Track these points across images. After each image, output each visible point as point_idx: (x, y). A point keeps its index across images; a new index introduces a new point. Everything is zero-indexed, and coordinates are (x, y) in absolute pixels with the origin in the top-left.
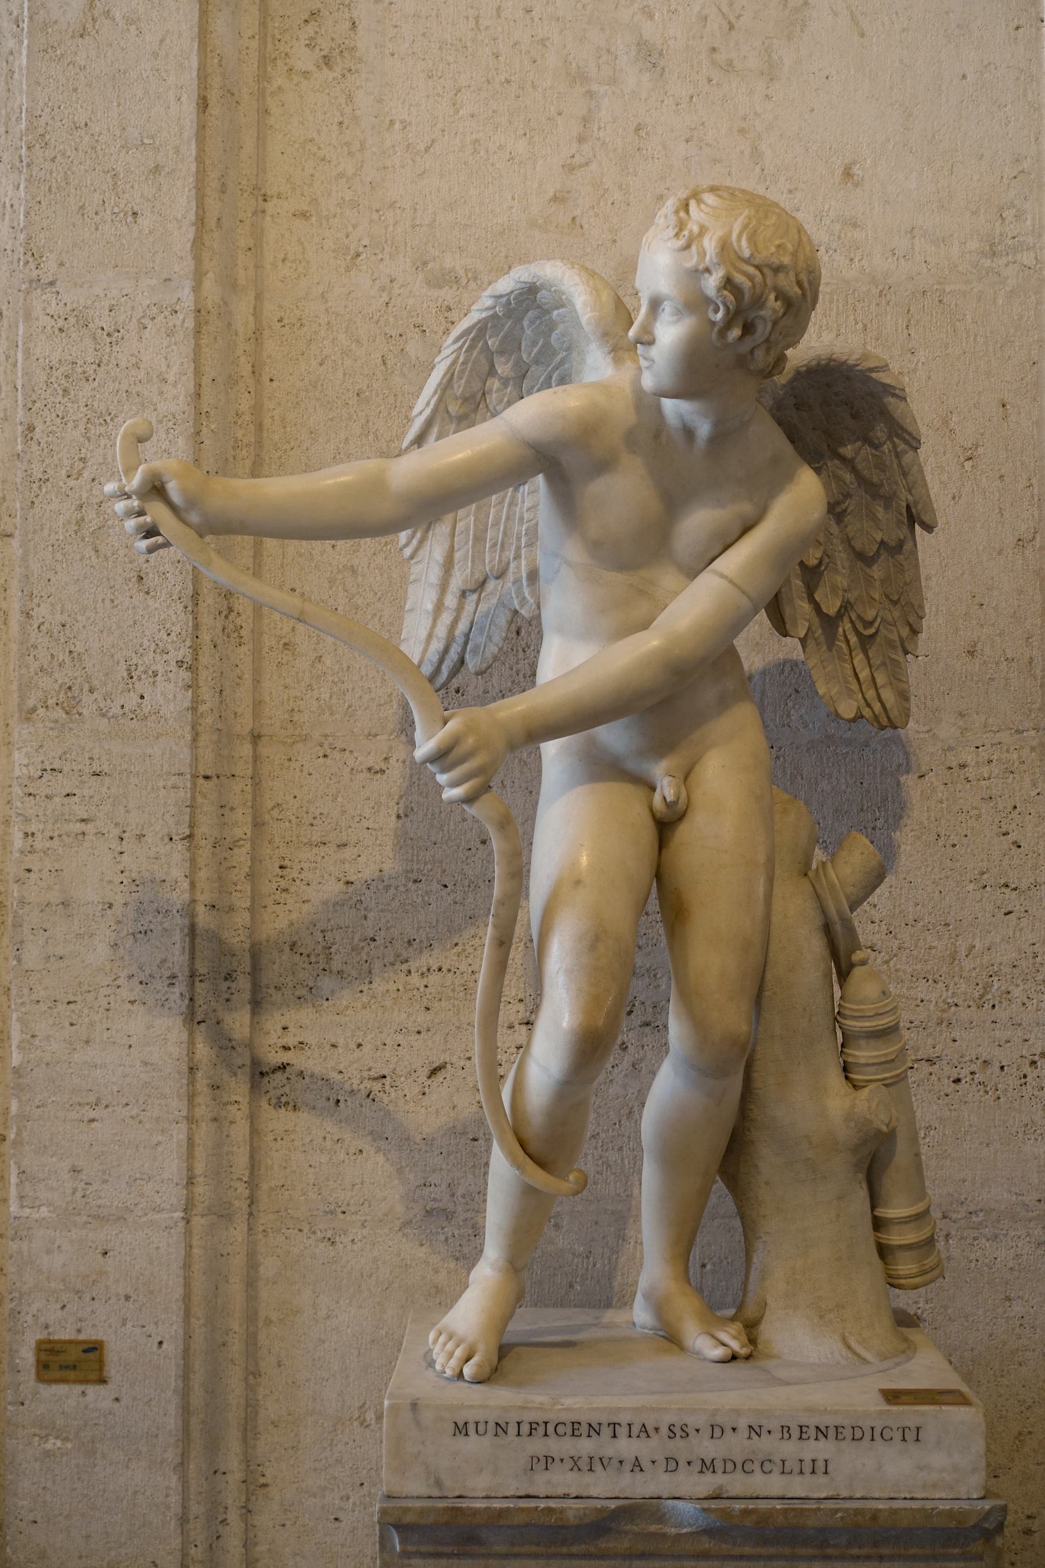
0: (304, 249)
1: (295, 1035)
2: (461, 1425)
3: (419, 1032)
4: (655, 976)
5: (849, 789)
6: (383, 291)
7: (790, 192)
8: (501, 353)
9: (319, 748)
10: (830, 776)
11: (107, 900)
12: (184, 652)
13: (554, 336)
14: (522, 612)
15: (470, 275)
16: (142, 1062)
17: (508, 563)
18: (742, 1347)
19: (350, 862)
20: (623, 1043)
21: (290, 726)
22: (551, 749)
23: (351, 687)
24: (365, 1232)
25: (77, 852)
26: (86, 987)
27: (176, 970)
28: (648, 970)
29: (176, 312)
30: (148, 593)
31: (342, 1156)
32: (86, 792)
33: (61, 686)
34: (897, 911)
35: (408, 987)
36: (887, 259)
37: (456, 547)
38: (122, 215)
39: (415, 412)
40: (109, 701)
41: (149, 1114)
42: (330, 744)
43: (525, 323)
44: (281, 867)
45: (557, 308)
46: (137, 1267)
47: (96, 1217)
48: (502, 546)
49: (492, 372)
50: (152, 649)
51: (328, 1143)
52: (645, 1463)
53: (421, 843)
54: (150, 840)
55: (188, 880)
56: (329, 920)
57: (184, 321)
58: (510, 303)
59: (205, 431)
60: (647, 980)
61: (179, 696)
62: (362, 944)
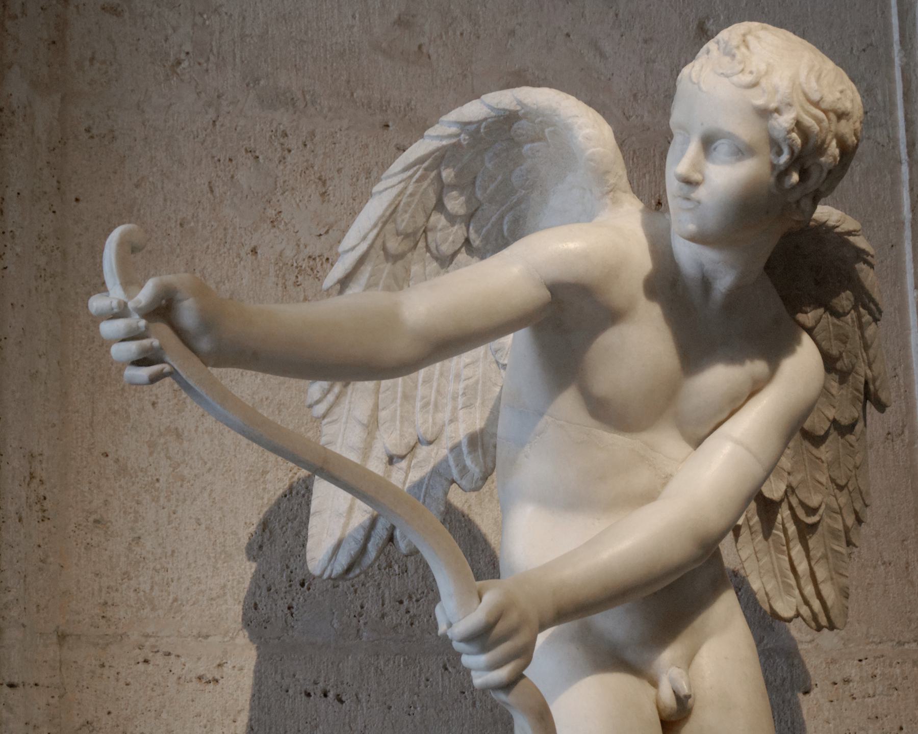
6: (209, 106)
7: (645, 41)
8: (453, 187)
9: (138, 651)
15: (308, 97)
17: (444, 425)
21: (103, 622)
42: (153, 646)
48: (436, 406)
49: (440, 206)
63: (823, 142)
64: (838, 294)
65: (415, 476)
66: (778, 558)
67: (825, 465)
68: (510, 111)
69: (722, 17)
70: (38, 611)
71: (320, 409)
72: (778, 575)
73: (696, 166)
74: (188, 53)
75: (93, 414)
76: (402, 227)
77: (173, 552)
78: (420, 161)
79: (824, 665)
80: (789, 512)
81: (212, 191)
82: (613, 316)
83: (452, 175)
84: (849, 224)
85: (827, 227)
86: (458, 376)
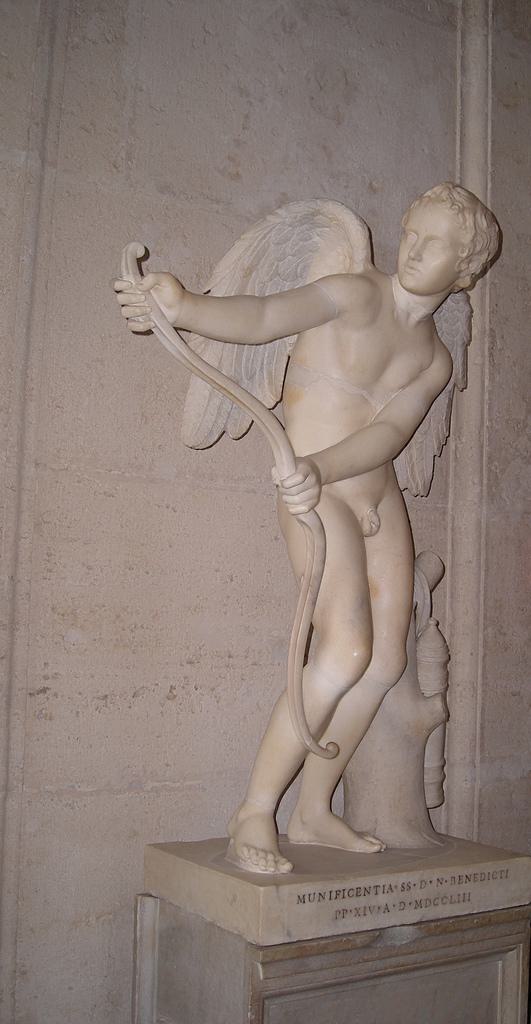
2: (301, 897)
52: (390, 907)
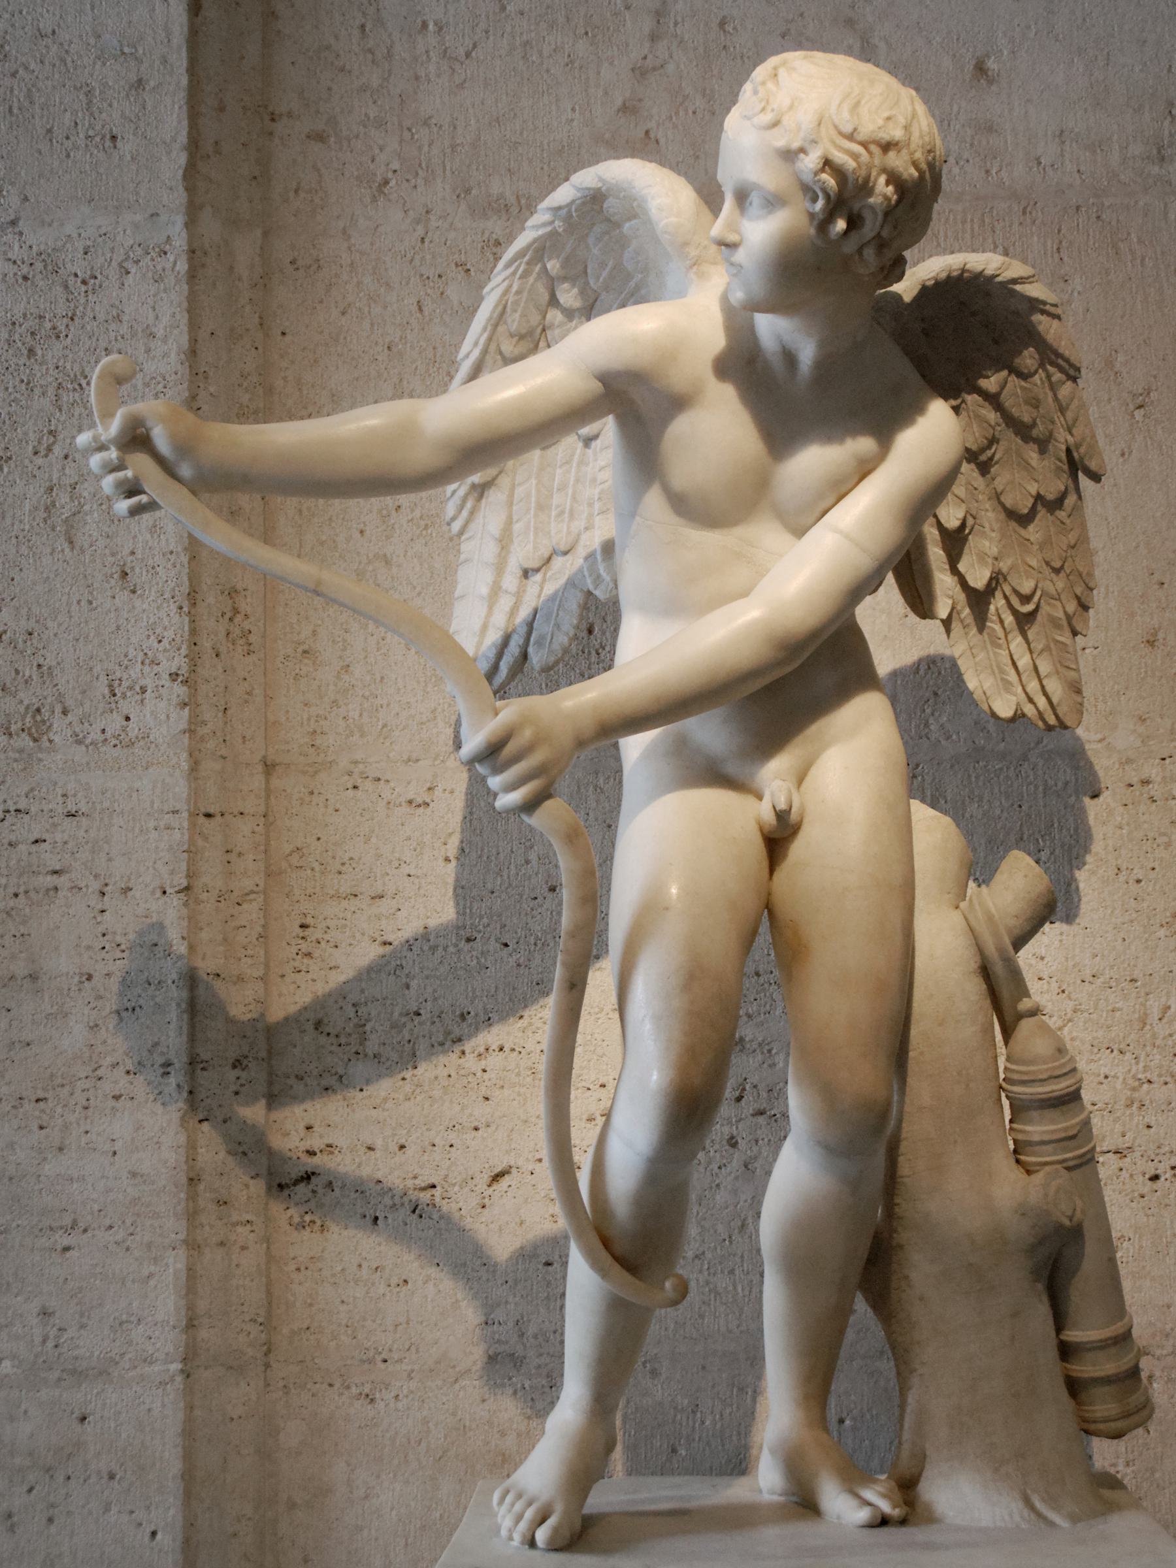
0: (320, 176)
1: (321, 1137)
3: (476, 1129)
4: (770, 1051)
5: (1005, 814)
6: (418, 223)
8: (564, 279)
9: (347, 777)
10: (981, 799)
11: (85, 970)
12: (179, 662)
13: (626, 255)
14: (597, 593)
15: (523, 201)
16: (129, 1172)
17: (579, 535)
18: (894, 1507)
19: (387, 918)
20: (732, 1137)
21: (312, 750)
22: (635, 747)
23: (385, 702)
24: (413, 1385)
25: (48, 912)
26: (59, 1081)
27: (172, 1056)
28: (760, 1045)
29: (165, 253)
30: (134, 592)
31: (382, 1289)
32: (59, 837)
33: (27, 708)
34: (1071, 963)
35: (462, 1072)
36: (1031, 169)
37: (515, 518)
38: (98, 139)
39: (461, 355)
40: (86, 724)
41: (138, 1238)
42: (362, 773)
43: (591, 240)
44: (302, 926)
45: (629, 219)
46: (124, 1436)
47: (73, 1372)
49: (553, 301)
50: (140, 661)
51: (365, 1272)
53: (475, 892)
54: (138, 895)
55: (186, 943)
56: (362, 991)
57: (175, 263)
58: (571, 216)
59: (202, 394)
60: (760, 1057)
61: (173, 716)
62: (404, 1020)
63: (867, 179)
64: (1020, 353)
65: (550, 589)
66: (995, 653)
67: (1036, 547)
68: (593, 189)
69: (1005, 53)
70: (244, 742)
71: (456, 526)
72: (996, 671)
73: (732, 226)
74: (395, 171)
75: (301, 546)
76: (514, 327)
77: (382, 678)
78: (521, 254)
79: (1117, 766)
80: (1004, 601)
81: (420, 309)
82: (678, 403)
83: (558, 266)
84: (1016, 269)
85: (985, 277)
86: (594, 480)
